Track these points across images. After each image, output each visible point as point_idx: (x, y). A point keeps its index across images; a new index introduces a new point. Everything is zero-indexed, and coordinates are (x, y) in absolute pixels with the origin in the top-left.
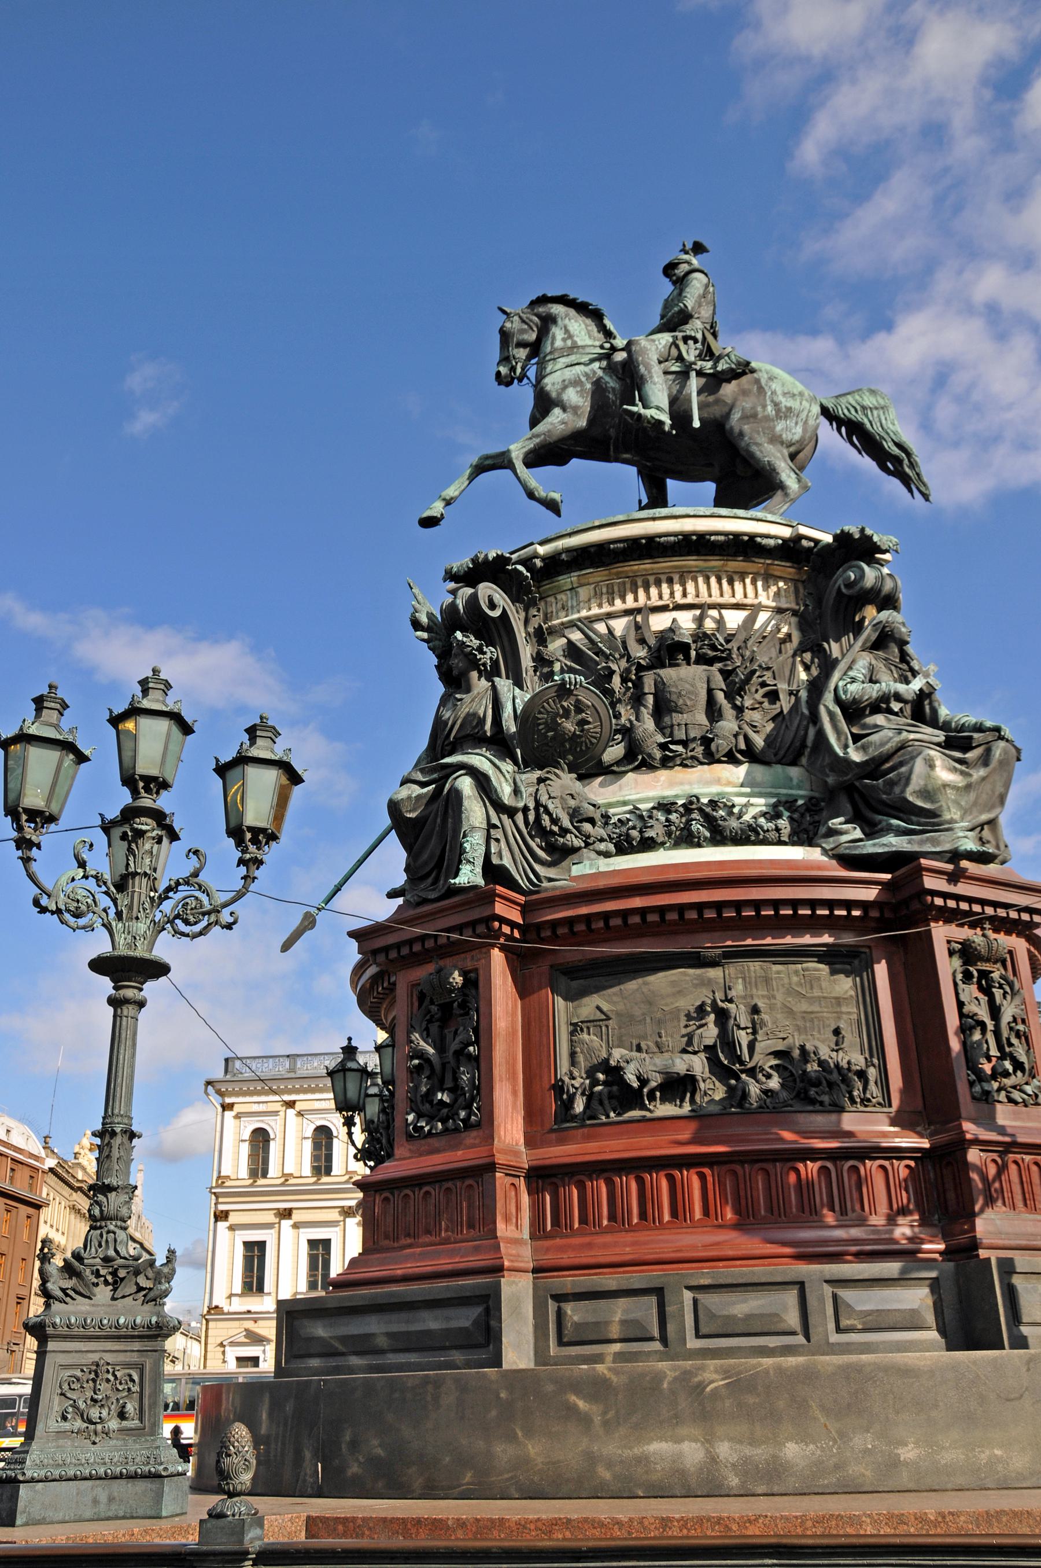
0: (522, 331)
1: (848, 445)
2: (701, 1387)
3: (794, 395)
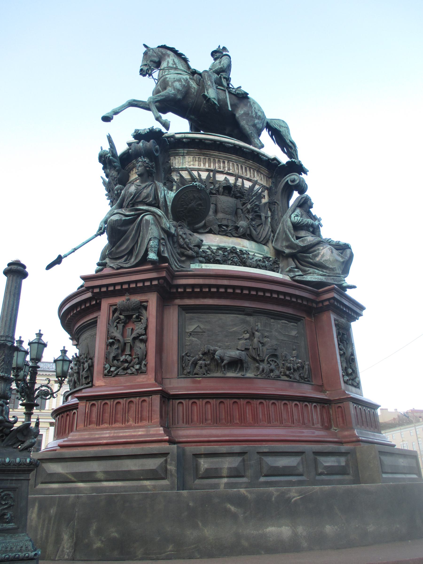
0: (154, 56)
1: (271, 138)
2: (289, 500)
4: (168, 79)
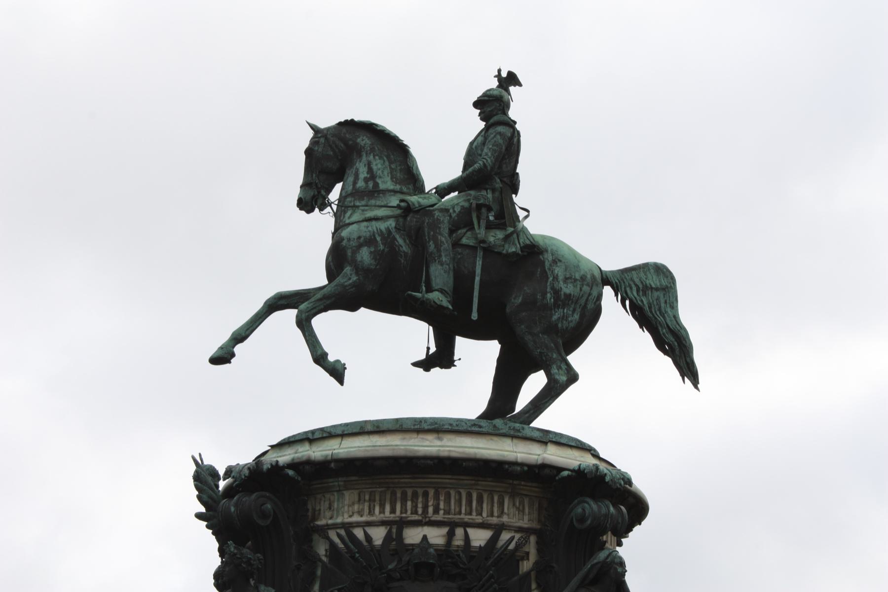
3: (576, 280)
4: (344, 243)
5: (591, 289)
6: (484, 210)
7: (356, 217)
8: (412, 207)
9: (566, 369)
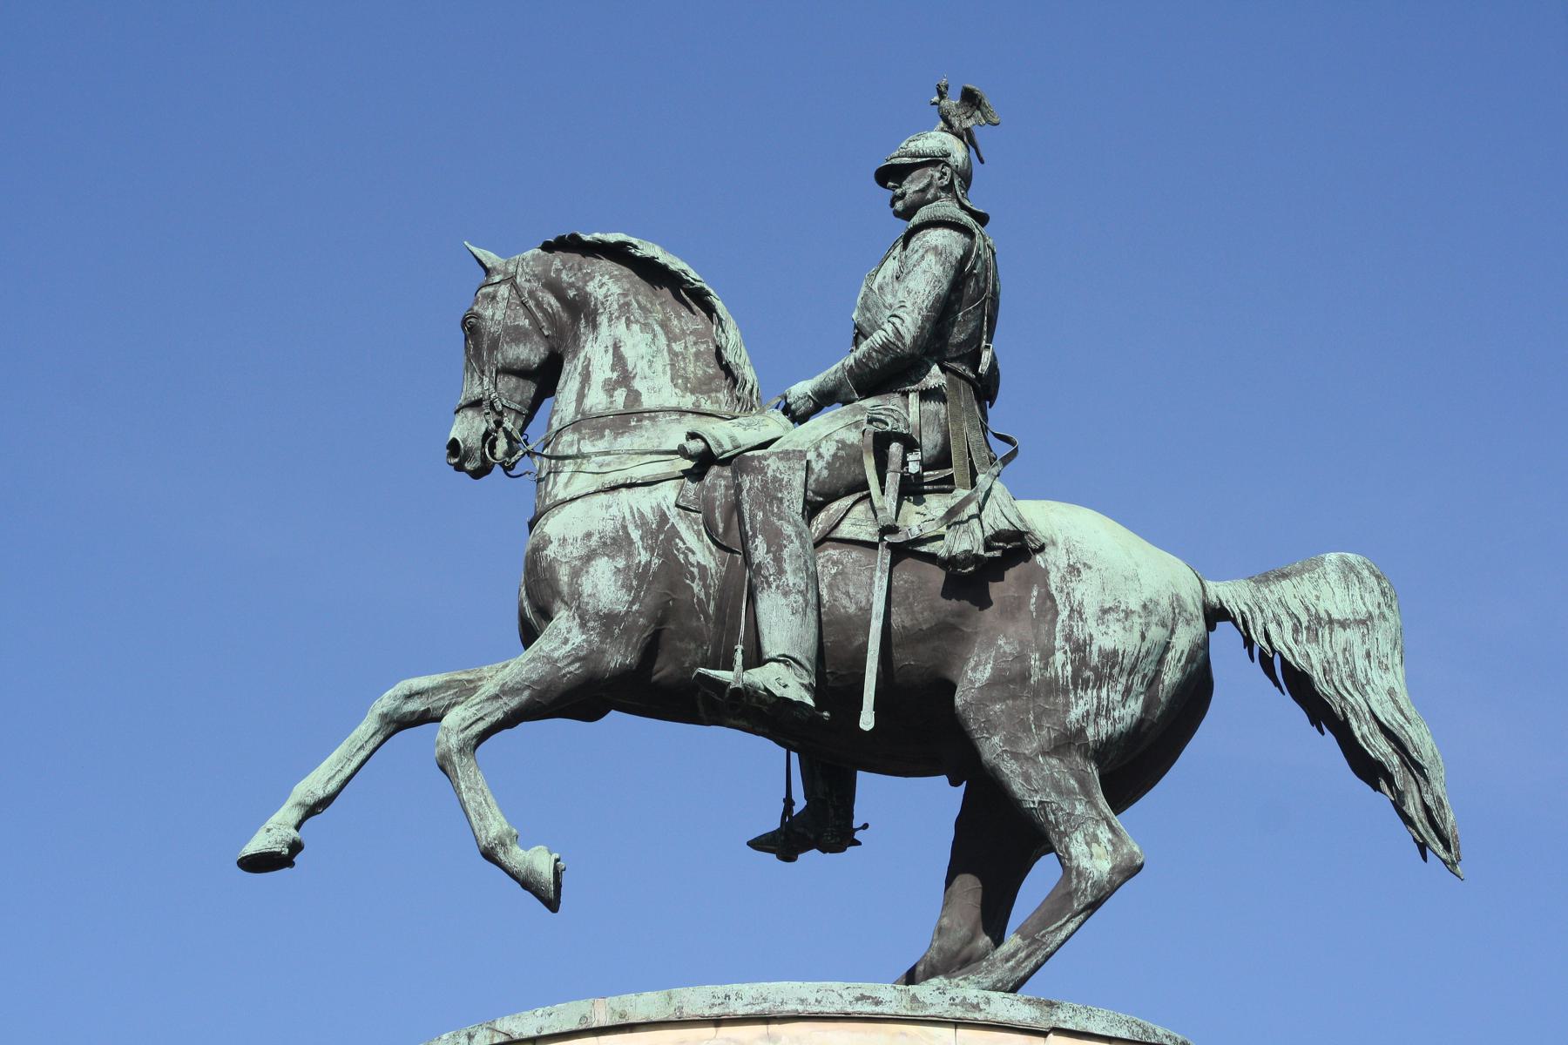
0: (518, 335)
3: (1128, 614)
5: (1173, 632)
6: (895, 448)
7: (582, 483)
8: (715, 450)
9: (1109, 840)
